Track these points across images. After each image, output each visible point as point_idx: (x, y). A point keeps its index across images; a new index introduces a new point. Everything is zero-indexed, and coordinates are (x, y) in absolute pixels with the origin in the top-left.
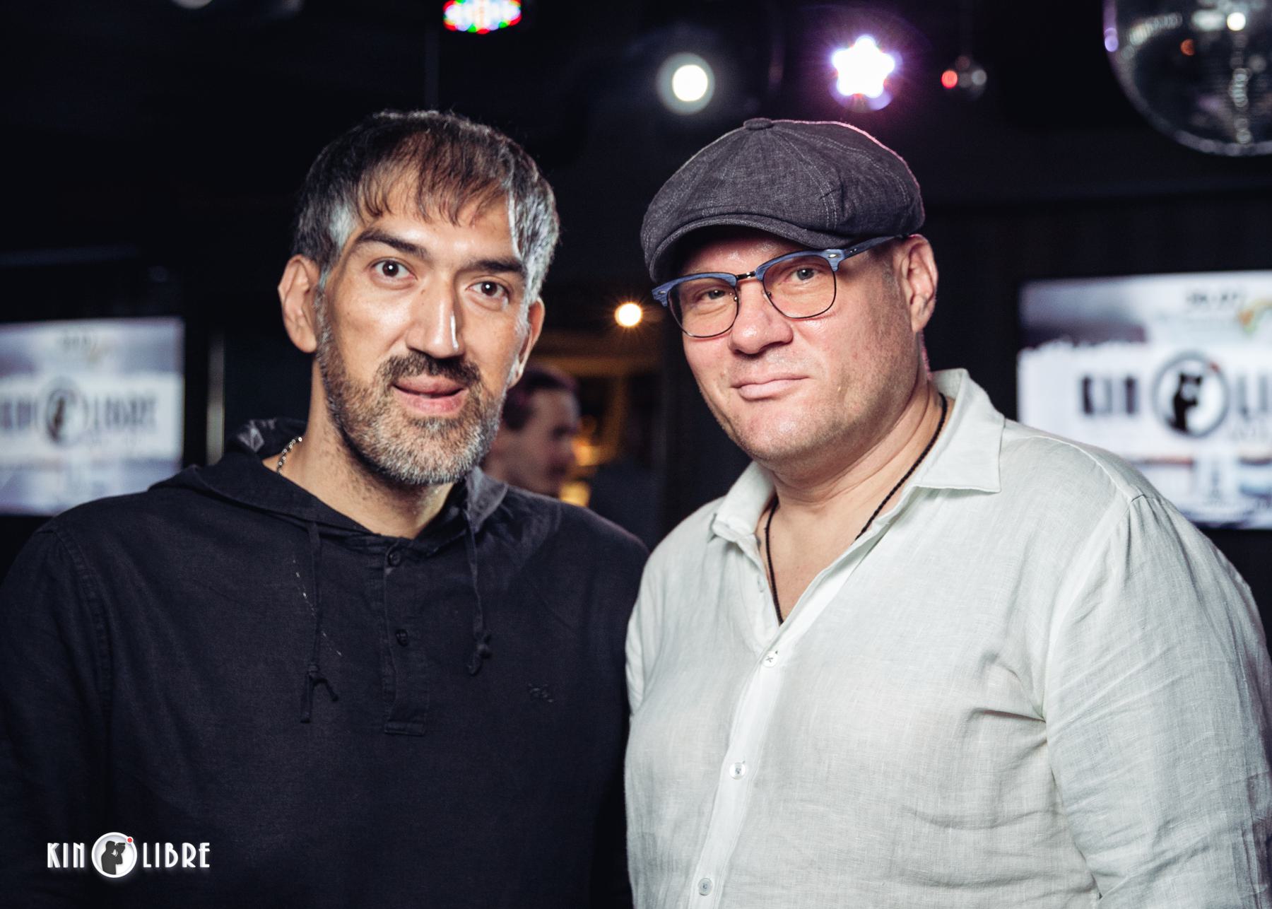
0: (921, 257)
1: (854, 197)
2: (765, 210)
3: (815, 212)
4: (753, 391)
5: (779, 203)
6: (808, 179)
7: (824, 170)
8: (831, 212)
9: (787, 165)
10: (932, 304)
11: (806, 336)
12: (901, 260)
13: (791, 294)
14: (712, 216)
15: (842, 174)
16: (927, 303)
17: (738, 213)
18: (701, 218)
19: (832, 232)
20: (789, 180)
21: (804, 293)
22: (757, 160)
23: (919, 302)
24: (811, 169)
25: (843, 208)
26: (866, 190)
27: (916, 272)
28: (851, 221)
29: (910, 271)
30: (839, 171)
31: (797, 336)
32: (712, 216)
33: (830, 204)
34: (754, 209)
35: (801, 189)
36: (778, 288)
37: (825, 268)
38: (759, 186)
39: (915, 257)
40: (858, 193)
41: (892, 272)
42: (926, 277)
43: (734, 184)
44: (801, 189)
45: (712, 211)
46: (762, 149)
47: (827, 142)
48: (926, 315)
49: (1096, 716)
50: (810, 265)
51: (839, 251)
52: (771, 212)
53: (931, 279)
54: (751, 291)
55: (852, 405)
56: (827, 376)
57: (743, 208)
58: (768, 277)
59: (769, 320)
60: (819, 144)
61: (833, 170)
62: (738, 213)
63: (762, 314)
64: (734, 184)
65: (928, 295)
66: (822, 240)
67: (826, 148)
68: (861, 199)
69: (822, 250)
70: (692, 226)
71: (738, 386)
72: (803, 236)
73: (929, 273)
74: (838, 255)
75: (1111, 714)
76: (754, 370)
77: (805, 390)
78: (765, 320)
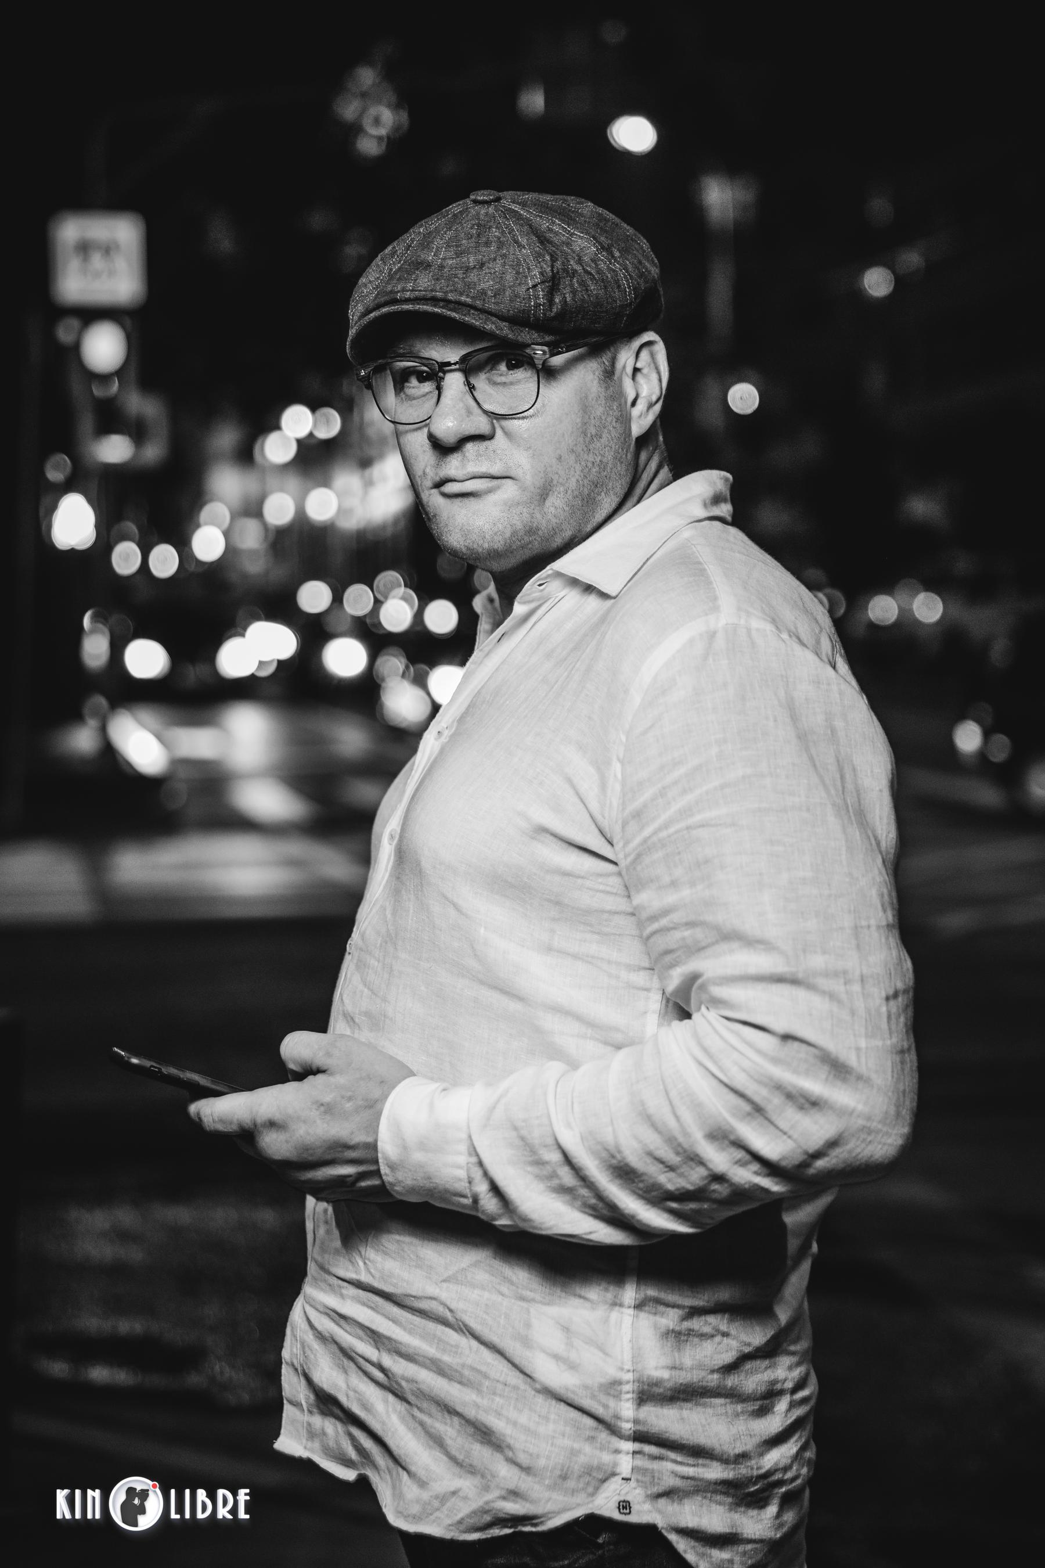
0: (653, 356)
1: (568, 290)
2: (463, 298)
3: (518, 304)
4: (451, 488)
5: (483, 292)
6: (519, 264)
7: (538, 256)
8: (537, 305)
9: (501, 245)
10: (658, 408)
11: (507, 434)
12: (625, 357)
13: (495, 384)
14: (407, 301)
15: (558, 264)
16: (651, 406)
17: (434, 301)
18: (395, 302)
19: (540, 325)
20: (498, 266)
21: (509, 389)
22: (469, 237)
23: (641, 406)
24: (526, 251)
25: (551, 302)
26: (583, 283)
27: (645, 371)
28: (562, 315)
29: (636, 370)
30: (554, 259)
31: (499, 433)
32: (407, 301)
33: (537, 297)
34: (451, 296)
35: (509, 277)
36: (480, 381)
37: (529, 362)
38: (467, 269)
39: (645, 354)
40: (572, 285)
41: (609, 374)
42: (654, 376)
43: (442, 267)
44: (509, 277)
45: (408, 295)
46: (479, 225)
47: (554, 223)
48: (650, 418)
49: (672, 830)
50: (515, 357)
51: (546, 348)
52: (469, 300)
53: (660, 380)
54: (454, 381)
55: (552, 509)
56: (528, 477)
57: (439, 294)
58: (469, 368)
59: (469, 412)
60: (545, 225)
61: (548, 258)
62: (434, 301)
63: (461, 405)
64: (442, 267)
65: (654, 398)
66: (525, 336)
67: (550, 230)
68: (574, 292)
69: (528, 346)
70: (385, 310)
71: (439, 485)
72: (504, 330)
73: (659, 373)
74: (544, 352)
75: (688, 828)
76: (453, 466)
77: (508, 491)
78: (463, 412)
